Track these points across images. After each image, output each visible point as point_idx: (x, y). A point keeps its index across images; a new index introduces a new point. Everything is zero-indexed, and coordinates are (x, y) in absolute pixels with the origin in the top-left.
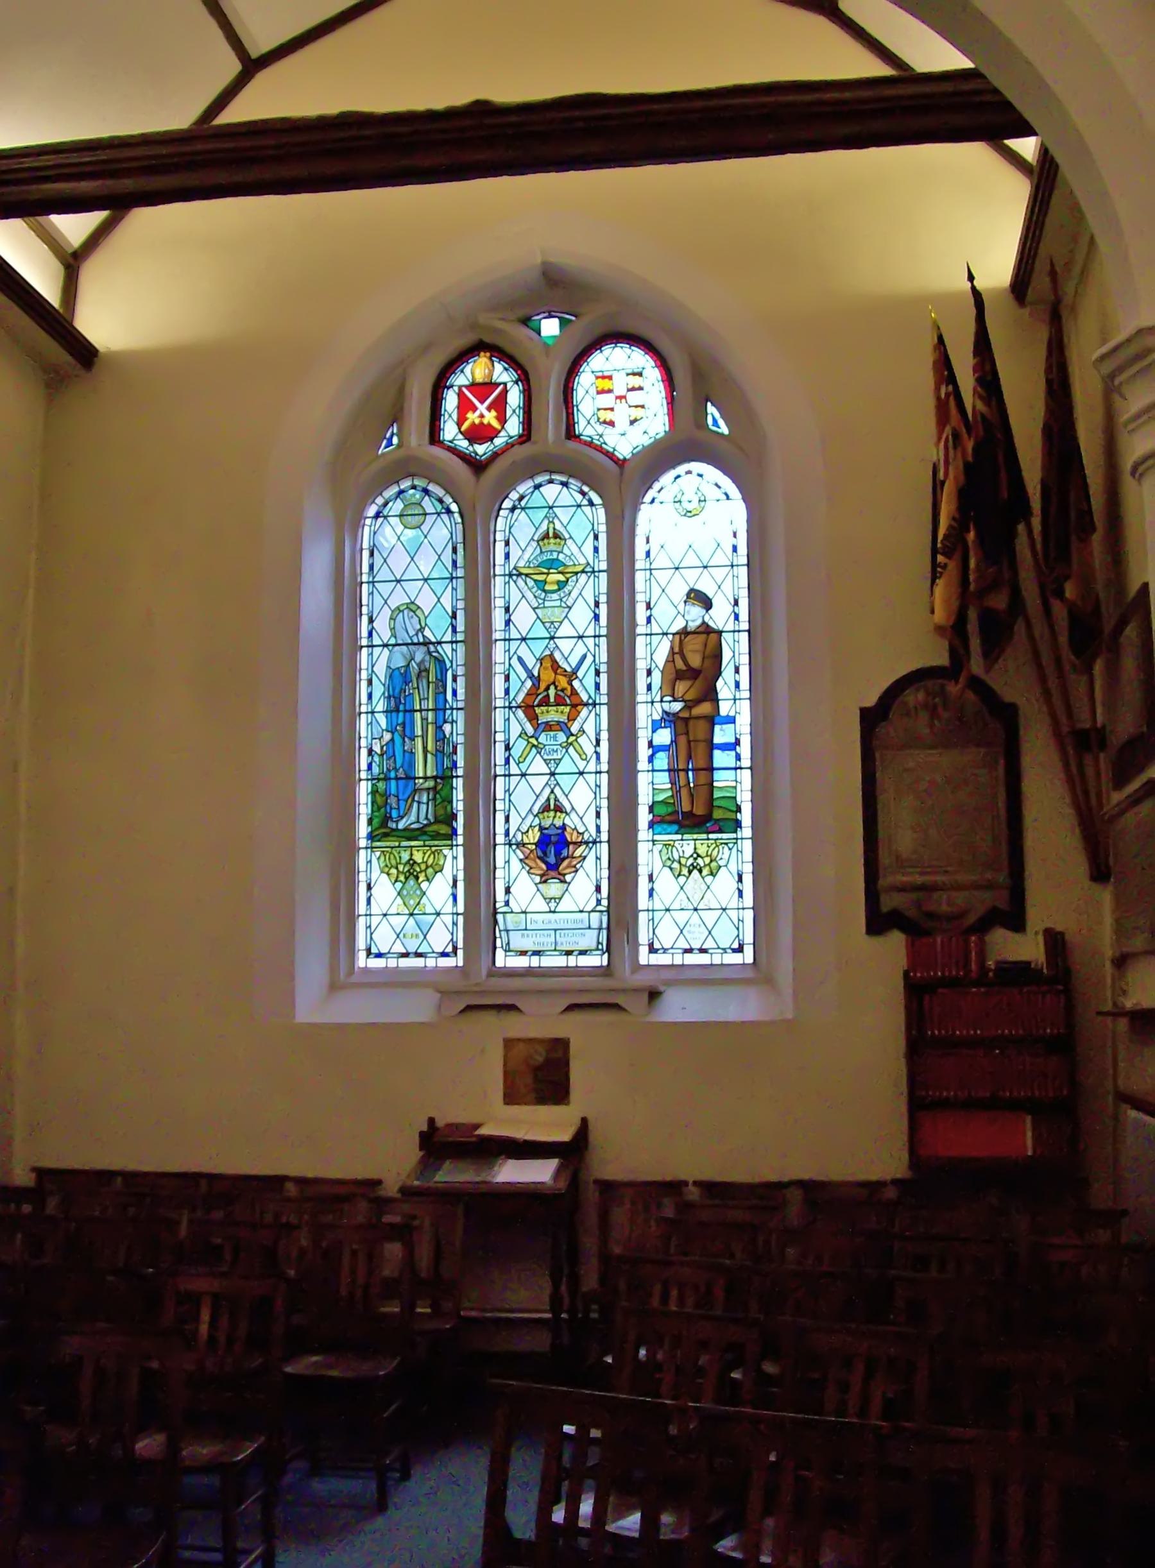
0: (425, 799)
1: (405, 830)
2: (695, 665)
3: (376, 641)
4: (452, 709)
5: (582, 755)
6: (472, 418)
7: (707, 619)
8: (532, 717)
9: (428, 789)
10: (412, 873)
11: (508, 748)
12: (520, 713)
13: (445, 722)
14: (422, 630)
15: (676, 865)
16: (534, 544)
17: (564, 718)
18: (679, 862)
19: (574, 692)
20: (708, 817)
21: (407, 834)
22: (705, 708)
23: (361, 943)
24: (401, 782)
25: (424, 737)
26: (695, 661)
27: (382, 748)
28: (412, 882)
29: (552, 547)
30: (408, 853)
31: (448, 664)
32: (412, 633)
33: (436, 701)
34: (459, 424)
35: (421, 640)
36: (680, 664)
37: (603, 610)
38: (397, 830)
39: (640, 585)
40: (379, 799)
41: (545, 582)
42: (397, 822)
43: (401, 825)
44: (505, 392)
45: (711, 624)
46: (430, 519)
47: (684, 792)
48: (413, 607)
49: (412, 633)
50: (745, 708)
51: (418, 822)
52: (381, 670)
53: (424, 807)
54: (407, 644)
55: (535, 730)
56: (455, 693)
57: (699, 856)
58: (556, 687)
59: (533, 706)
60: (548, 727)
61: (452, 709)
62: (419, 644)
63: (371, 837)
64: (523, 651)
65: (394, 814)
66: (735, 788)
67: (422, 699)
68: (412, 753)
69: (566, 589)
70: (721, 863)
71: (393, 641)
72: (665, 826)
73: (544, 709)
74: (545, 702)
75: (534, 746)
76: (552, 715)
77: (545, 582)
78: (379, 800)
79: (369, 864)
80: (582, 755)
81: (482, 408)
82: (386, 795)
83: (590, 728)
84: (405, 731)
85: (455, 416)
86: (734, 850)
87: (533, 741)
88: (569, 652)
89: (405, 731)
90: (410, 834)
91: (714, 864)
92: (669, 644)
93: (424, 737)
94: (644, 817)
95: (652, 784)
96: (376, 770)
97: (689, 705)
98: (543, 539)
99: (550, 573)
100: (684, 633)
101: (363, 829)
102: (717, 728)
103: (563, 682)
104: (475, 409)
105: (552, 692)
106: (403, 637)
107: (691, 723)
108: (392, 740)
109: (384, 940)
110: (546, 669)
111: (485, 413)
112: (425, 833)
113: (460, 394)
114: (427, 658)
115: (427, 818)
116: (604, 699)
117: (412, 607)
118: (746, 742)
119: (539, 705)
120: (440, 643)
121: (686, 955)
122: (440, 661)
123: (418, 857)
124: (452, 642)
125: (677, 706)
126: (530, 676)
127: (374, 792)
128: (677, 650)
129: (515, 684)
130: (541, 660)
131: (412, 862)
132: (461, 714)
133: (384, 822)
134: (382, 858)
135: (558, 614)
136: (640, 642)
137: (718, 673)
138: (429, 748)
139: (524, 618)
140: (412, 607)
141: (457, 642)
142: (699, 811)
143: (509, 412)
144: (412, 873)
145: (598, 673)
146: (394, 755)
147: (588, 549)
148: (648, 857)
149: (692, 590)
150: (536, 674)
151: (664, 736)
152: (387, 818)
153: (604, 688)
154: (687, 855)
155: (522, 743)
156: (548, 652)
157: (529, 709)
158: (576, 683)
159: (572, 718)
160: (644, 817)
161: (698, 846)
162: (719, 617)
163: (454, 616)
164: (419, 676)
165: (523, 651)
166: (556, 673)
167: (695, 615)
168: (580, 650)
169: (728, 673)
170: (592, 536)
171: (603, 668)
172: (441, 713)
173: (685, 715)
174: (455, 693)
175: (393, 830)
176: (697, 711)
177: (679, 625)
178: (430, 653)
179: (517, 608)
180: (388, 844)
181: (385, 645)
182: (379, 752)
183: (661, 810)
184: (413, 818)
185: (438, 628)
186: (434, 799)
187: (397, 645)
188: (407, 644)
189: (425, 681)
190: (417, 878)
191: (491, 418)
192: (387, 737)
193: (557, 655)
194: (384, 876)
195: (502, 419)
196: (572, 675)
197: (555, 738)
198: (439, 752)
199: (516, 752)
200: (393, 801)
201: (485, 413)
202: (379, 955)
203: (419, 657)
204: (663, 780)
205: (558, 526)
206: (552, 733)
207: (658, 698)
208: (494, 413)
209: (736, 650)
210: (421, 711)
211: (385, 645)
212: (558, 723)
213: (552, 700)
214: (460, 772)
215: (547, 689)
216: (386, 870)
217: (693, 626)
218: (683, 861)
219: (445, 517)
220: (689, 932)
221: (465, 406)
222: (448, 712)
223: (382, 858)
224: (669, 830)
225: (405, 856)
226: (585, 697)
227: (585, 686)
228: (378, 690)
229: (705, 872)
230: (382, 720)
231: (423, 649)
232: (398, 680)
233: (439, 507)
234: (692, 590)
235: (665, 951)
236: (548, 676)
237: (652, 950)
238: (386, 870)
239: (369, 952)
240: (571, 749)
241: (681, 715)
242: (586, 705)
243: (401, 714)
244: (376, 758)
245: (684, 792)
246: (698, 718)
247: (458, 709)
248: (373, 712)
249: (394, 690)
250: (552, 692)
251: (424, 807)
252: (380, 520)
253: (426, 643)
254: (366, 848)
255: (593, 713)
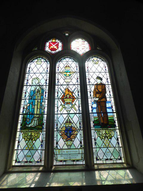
0: (36, 120)
1: (31, 127)
2: (100, 91)
3: (28, 84)
4: (45, 99)
5: (75, 109)
6: (52, 47)
7: (101, 82)
8: (63, 101)
9: (37, 117)
10: (31, 139)
11: (58, 108)
12: (61, 100)
13: (43, 102)
14: (39, 83)
15: (101, 136)
16: (64, 68)
17: (71, 101)
18: (102, 135)
19: (73, 96)
20: (108, 124)
21: (31, 128)
22: (103, 100)
23: (14, 158)
24: (31, 115)
25: (37, 105)
26: (100, 90)
27: (27, 107)
28: (31, 141)
29: (68, 68)
30: (30, 133)
31: (44, 90)
32: (37, 83)
33: (41, 97)
34: (49, 48)
35: (39, 85)
36: (97, 91)
37: (79, 80)
38: (28, 127)
39: (87, 76)
40: (24, 120)
41: (66, 74)
42: (28, 125)
43: (29, 126)
44: (58, 44)
45: (102, 83)
46: (43, 63)
47: (101, 118)
48: (38, 79)
49: (37, 83)
50: (112, 99)
51: (34, 125)
52: (29, 90)
53: (36, 121)
54: (35, 86)
55: (64, 104)
56: (45, 95)
57: (107, 134)
58: (69, 95)
59: (64, 99)
60: (67, 103)
61: (45, 99)
62: (38, 86)
63: (21, 129)
64: (61, 87)
65: (28, 123)
66: (113, 117)
67: (38, 96)
68: (34, 109)
69: (71, 76)
70: (113, 135)
71: (32, 85)
72: (97, 126)
73: (66, 99)
74: (67, 98)
75: (64, 107)
76: (68, 101)
77: (66, 74)
78: (24, 119)
79: (19, 135)
80: (75, 109)
81: (54, 46)
82: (26, 118)
83: (77, 103)
84: (32, 104)
85: (48, 46)
86: (115, 132)
87: (64, 106)
88: (72, 88)
89: (32, 104)
90: (31, 128)
91: (110, 136)
92: (94, 87)
93: (37, 105)
94: (92, 124)
95: (94, 117)
96: (25, 112)
97: (100, 99)
98: (66, 67)
99: (67, 73)
100: (97, 85)
101: (19, 127)
102: (107, 104)
103: (71, 94)
104: (52, 46)
105: (68, 96)
106: (34, 84)
107: (101, 103)
108: (30, 105)
109: (21, 157)
110: (67, 91)
111: (54, 46)
112: (35, 128)
113: (49, 43)
114: (40, 88)
115: (36, 124)
116: (80, 97)
117: (37, 78)
118: (114, 107)
119: (65, 98)
120: (43, 86)
121: (106, 161)
122: (43, 89)
123: (33, 134)
124: (45, 86)
125: (97, 99)
126: (63, 92)
127: (23, 118)
128: (96, 88)
129: (59, 94)
130: (65, 89)
131: (31, 136)
132: (47, 100)
133: (25, 125)
134: (23, 134)
135: (69, 81)
136: (88, 86)
137: (106, 92)
138: (38, 107)
139: (62, 81)
140: (37, 78)
141: (109, 85)
142: (105, 123)
143: (59, 46)
144: (31, 139)
145: (78, 92)
146: (30, 109)
147: (75, 69)
148: (94, 134)
149: (98, 77)
150: (64, 92)
151: (95, 106)
152: (25, 125)
153: (80, 95)
154: (104, 133)
155: (61, 107)
156: (67, 88)
157: (63, 99)
158: (73, 94)
159: (73, 101)
160: (92, 124)
161: (106, 131)
162: (104, 81)
163: (46, 80)
164: (37, 92)
165: (61, 87)
166: (69, 92)
167: (99, 81)
168: (74, 87)
169: (108, 92)
170: (76, 67)
171: (79, 91)
172: (42, 100)
173: (99, 101)
174: (45, 95)
175: (27, 127)
176: (102, 100)
177: (96, 83)
178: (40, 88)
179: (60, 79)
180: (25, 131)
181: (30, 86)
182: (26, 108)
183: (96, 123)
184: (33, 124)
185: (43, 82)
186: (39, 120)
187: (33, 86)
188: (35, 86)
189: (39, 93)
190: (32, 140)
191: (55, 47)
192: (28, 105)
193: (69, 88)
194: (23, 139)
195: (58, 48)
196: (72, 93)
197: (69, 106)
198: (41, 108)
199: (60, 109)
200: (28, 120)
201: (54, 46)
202: (19, 162)
203: (38, 88)
204: (96, 115)
205: (69, 65)
206: (68, 105)
207: (93, 97)
208: (56, 46)
209: (109, 89)
210: (37, 99)
211: (30, 86)
212: (70, 102)
213: (68, 97)
214: (46, 113)
215: (67, 95)
216: (24, 137)
217: (99, 83)
218: (103, 135)
219: (46, 62)
220: (107, 154)
221: (50, 45)
222: (44, 100)
223: (23, 134)
224: (98, 127)
225: (30, 134)
226: (76, 97)
227: (76, 94)
228: (27, 94)
229: (109, 138)
230: (27, 101)
231: (39, 87)
232: (32, 93)
233: (45, 61)
234: (98, 77)
235: (101, 160)
236: (67, 93)
237: (97, 160)
238: (24, 137)
239: (16, 161)
240: (73, 108)
241: (98, 101)
242: (76, 98)
243: (32, 100)
244: (25, 109)
245: (101, 118)
246: (102, 102)
247: (46, 99)
248: (25, 99)
249: (31, 94)
250: (68, 96)
251: (36, 121)
252: (32, 62)
253: (40, 86)
254: (20, 131)
255: (78, 100)
